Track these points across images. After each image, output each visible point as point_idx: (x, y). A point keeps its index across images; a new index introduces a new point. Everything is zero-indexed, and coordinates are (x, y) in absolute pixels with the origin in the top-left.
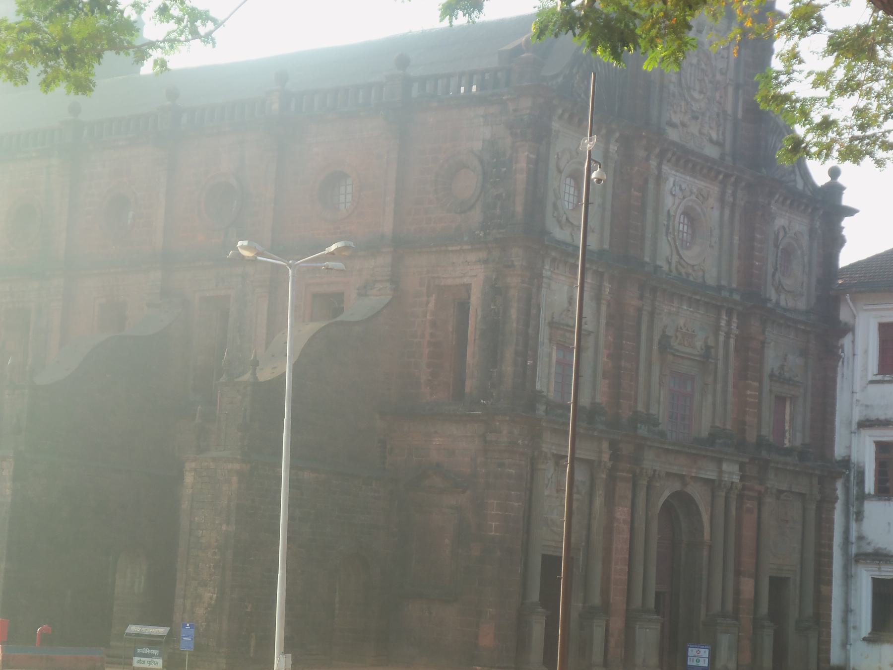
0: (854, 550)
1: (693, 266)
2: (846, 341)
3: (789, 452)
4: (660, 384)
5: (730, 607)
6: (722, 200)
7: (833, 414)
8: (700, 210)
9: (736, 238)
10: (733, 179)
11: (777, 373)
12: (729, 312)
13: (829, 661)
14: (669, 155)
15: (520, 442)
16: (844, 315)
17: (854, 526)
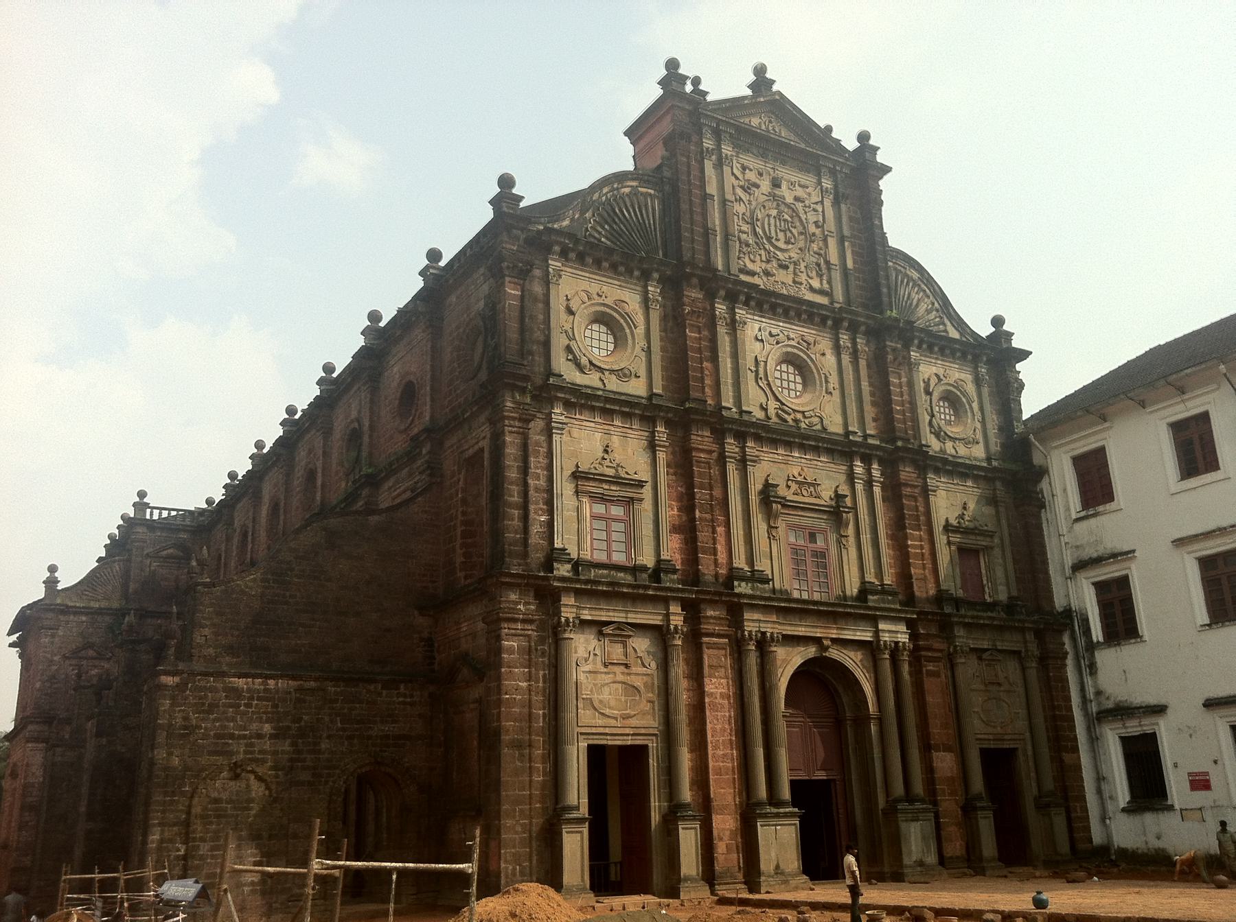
0: (1094, 708)
1: (803, 412)
2: (1044, 485)
3: (993, 606)
4: (769, 538)
5: (919, 788)
6: (837, 349)
7: (1045, 562)
8: (805, 357)
9: (865, 385)
10: (846, 324)
11: (954, 522)
12: (867, 460)
13: (1090, 840)
14: (742, 298)
15: (521, 607)
16: (1037, 460)
17: (1089, 681)
